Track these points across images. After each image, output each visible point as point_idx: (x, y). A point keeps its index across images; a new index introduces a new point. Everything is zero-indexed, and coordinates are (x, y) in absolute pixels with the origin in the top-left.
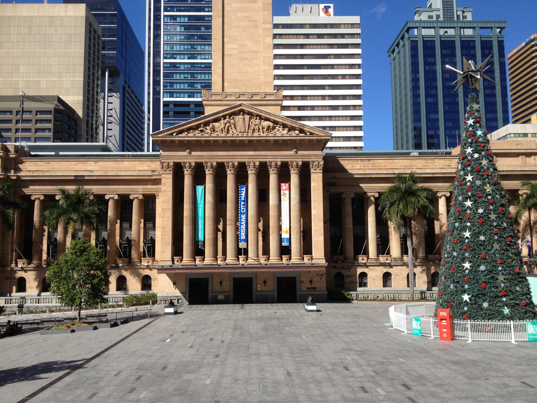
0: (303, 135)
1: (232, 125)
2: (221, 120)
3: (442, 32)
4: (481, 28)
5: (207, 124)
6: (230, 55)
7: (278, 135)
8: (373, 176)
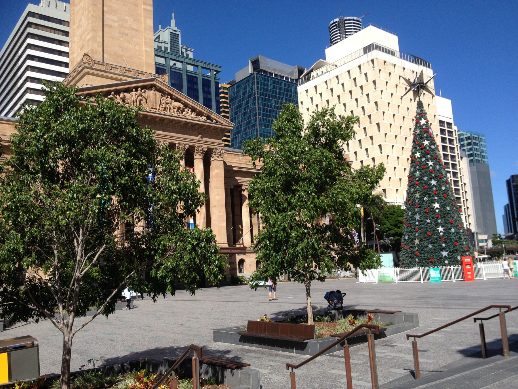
0: (210, 121)
1: (144, 99)
2: (132, 91)
3: (172, 63)
4: (202, 67)
5: (118, 92)
6: (110, 26)
7: (188, 117)
8: (249, 170)
